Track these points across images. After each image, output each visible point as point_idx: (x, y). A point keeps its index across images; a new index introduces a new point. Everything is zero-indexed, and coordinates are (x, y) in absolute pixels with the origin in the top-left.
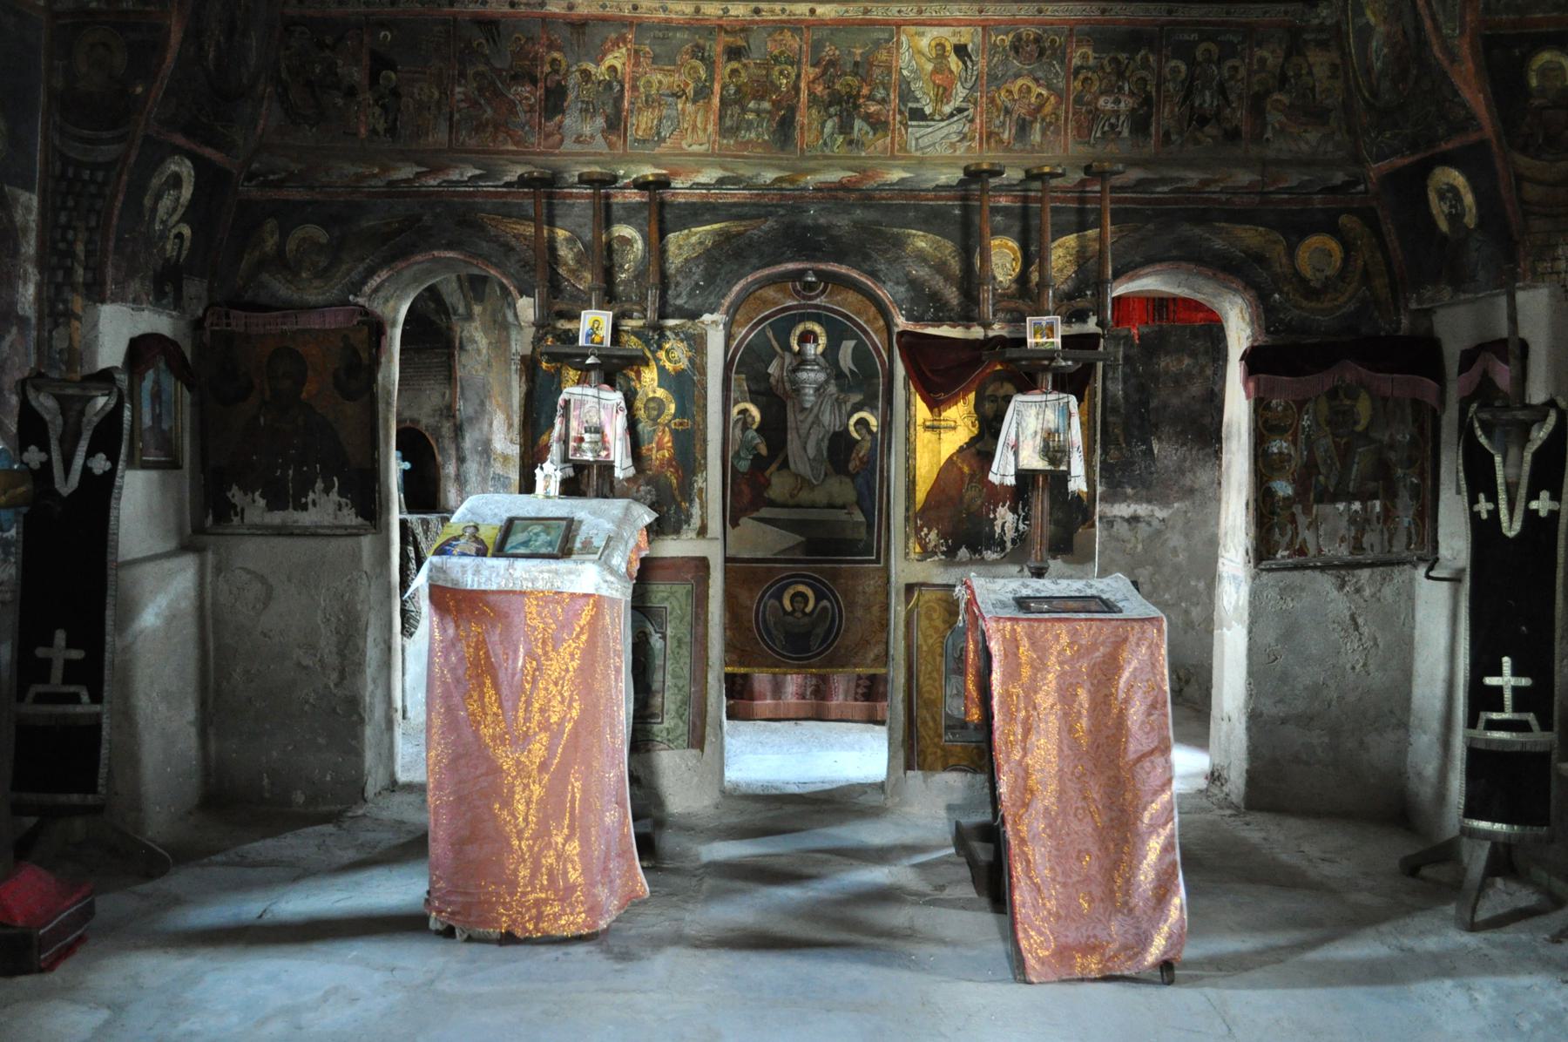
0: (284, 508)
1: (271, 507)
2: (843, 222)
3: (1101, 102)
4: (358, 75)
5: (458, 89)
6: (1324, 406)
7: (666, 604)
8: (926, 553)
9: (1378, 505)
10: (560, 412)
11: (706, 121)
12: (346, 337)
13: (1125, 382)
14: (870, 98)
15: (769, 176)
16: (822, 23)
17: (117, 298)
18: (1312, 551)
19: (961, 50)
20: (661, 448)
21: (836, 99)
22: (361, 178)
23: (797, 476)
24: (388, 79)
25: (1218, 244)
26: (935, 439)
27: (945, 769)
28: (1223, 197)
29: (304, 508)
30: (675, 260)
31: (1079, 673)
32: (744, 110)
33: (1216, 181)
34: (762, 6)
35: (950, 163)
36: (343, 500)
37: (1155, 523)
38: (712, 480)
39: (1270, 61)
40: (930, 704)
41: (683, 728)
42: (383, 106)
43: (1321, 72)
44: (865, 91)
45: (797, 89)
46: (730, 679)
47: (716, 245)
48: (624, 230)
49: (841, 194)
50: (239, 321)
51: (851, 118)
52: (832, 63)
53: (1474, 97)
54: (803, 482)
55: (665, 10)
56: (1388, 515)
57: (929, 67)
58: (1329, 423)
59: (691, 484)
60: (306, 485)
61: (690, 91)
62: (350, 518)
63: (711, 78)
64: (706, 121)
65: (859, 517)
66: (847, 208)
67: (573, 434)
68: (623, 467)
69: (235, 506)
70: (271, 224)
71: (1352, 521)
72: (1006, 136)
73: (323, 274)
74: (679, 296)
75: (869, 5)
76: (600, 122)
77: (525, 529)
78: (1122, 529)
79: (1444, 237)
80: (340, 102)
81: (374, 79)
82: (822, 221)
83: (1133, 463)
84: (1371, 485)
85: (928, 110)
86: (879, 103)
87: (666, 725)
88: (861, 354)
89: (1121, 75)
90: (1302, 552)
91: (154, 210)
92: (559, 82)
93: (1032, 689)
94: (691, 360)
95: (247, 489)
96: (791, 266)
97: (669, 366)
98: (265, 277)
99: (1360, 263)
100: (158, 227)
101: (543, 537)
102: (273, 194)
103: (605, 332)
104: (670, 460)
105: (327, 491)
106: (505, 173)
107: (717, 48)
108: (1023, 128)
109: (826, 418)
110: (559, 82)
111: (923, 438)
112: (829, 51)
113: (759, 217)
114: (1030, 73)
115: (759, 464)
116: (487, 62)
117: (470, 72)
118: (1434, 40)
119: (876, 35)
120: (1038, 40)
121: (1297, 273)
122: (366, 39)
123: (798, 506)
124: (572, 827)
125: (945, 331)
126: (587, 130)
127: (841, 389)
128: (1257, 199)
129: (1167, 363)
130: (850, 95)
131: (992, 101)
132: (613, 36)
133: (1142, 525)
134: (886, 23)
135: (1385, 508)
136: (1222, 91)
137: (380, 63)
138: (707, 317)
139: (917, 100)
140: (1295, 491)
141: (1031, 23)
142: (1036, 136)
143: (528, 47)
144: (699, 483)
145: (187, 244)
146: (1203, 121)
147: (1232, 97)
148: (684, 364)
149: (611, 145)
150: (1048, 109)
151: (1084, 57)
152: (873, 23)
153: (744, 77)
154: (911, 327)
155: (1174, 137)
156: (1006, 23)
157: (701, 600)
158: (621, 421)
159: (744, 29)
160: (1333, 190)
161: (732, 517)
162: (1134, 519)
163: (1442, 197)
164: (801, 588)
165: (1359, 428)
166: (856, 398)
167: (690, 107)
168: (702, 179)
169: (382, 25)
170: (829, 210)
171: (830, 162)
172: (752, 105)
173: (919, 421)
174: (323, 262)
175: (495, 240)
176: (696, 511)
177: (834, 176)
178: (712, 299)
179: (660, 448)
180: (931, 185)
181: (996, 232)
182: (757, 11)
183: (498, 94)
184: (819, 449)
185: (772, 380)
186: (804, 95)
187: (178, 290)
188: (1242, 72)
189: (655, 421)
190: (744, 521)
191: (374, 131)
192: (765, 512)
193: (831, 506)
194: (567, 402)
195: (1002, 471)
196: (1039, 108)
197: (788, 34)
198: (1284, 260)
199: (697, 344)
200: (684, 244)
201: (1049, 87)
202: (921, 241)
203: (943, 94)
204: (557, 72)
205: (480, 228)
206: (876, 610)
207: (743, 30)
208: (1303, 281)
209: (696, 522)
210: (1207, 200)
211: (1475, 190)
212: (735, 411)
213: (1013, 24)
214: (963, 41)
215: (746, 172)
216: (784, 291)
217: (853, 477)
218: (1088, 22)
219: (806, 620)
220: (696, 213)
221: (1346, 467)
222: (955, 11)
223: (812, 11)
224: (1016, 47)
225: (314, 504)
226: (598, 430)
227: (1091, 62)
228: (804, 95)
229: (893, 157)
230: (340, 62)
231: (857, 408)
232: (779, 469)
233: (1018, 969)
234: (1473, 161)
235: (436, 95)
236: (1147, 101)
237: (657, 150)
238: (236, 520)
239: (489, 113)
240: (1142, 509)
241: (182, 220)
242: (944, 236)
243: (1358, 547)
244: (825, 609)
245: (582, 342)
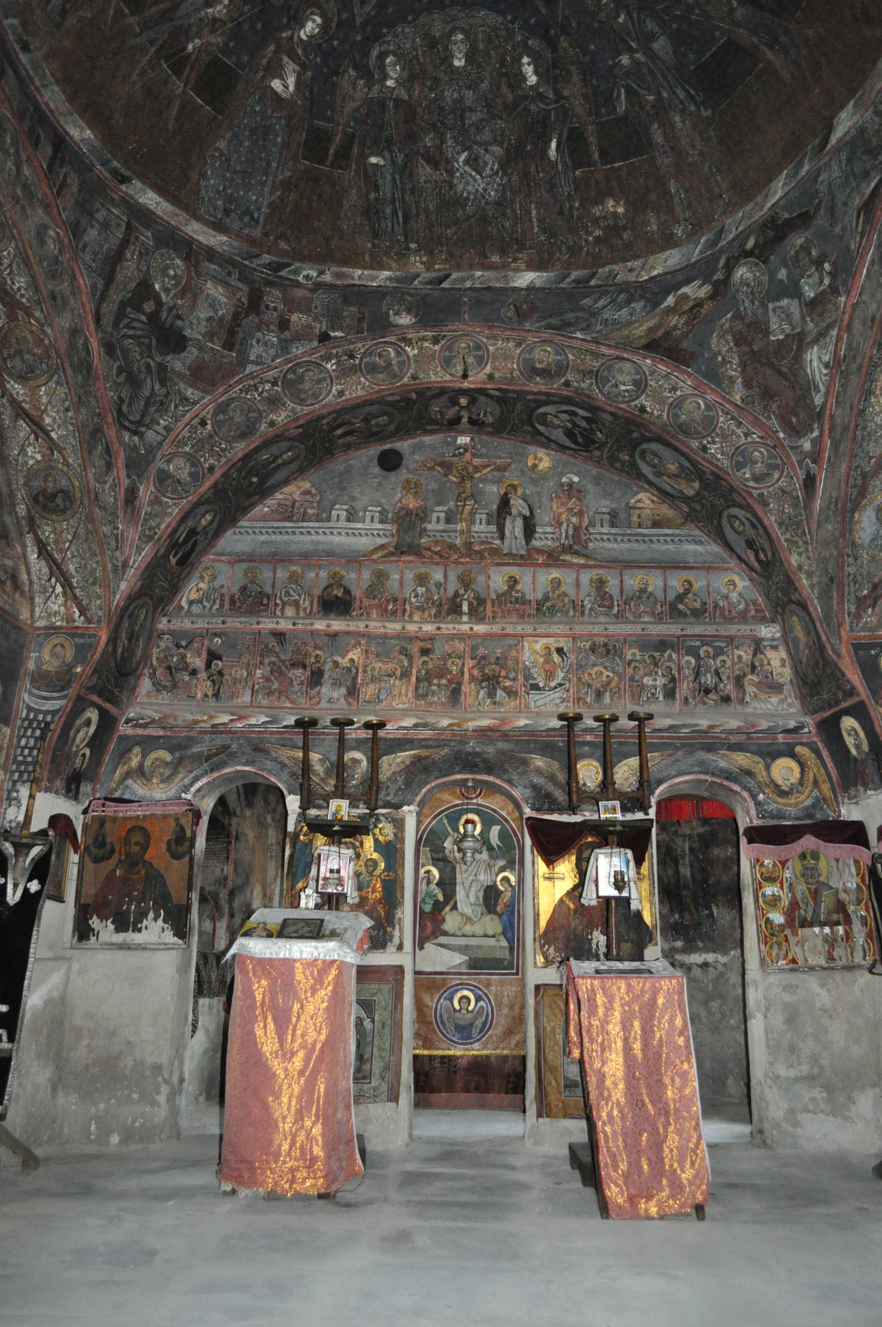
0: (126, 931)
1: (118, 930)
2: (490, 750)
3: (645, 680)
4: (198, 662)
5: (258, 671)
6: (799, 866)
7: (375, 998)
8: (548, 963)
9: (841, 930)
10: (315, 861)
11: (407, 692)
12: (177, 820)
13: (691, 867)
14: (506, 677)
15: (445, 722)
16: (477, 636)
17: (47, 790)
18: (801, 961)
19: (560, 651)
21: (486, 678)
22: (197, 722)
23: (462, 915)
24: (217, 665)
25: (722, 764)
26: (550, 887)
27: (565, 1117)
28: (723, 736)
29: (140, 930)
31: (631, 1011)
32: (430, 684)
33: (718, 726)
34: (443, 626)
36: (166, 926)
37: (720, 967)
38: (406, 913)
39: (745, 657)
40: (553, 1069)
41: (384, 1088)
42: (213, 681)
43: (776, 663)
44: (503, 673)
45: (462, 672)
46: (416, 1057)
47: (413, 763)
49: (489, 733)
50: (111, 809)
51: (495, 689)
52: (483, 658)
53: (854, 677)
54: (468, 919)
55: (384, 627)
56: (848, 936)
57: (541, 660)
58: (803, 876)
59: (394, 915)
60: (143, 915)
61: (398, 673)
62: (169, 937)
63: (411, 665)
64: (407, 692)
65: (504, 943)
66: (492, 742)
67: (322, 875)
68: (353, 897)
69: (93, 930)
70: (137, 750)
71: (825, 939)
72: (589, 700)
73: (166, 780)
74: (388, 794)
75: (505, 626)
76: (343, 691)
77: (295, 924)
78: (697, 972)
79: (855, 758)
80: (187, 678)
81: (208, 665)
82: (478, 749)
83: (700, 924)
84: (835, 917)
85: (541, 685)
86: (511, 680)
87: (373, 1084)
88: (503, 835)
89: (656, 665)
90: (794, 961)
91: (74, 739)
92: (319, 668)
93: (605, 1022)
94: (395, 834)
95: (103, 918)
96: (459, 777)
97: (381, 838)
98: (129, 782)
99: (811, 775)
100: (74, 749)
101: (306, 929)
102: (140, 731)
104: (380, 899)
105: (155, 919)
106: (283, 720)
107: (415, 649)
108: (599, 695)
110: (319, 668)
111: (543, 886)
112: (481, 651)
113: (439, 747)
114: (602, 664)
115: (438, 907)
116: (277, 656)
117: (267, 661)
118: (828, 647)
119: (508, 642)
120: (605, 645)
121: (772, 781)
122: (206, 643)
123: (464, 936)
124: (317, 1115)
125: (555, 817)
126: (335, 695)
127: (492, 857)
128: (744, 736)
129: (716, 852)
130: (494, 676)
131: (580, 679)
132: (353, 642)
133: (711, 969)
134: (515, 636)
135: (847, 933)
136: (717, 674)
137: (213, 656)
138: (406, 808)
139: (534, 679)
140: (786, 920)
141: (602, 636)
142: (607, 699)
143: (302, 648)
144: (399, 915)
145: (87, 760)
146: (707, 691)
147: (724, 678)
148: (391, 837)
149: (349, 704)
150: (614, 684)
151: (634, 654)
152: (508, 635)
153: (430, 666)
154: (534, 814)
155: (690, 700)
156: (587, 635)
157: (398, 996)
159: (431, 638)
160: (789, 731)
161: (420, 943)
162: (705, 965)
163: (849, 734)
164: (466, 993)
165: (822, 879)
166: (501, 863)
167: (398, 682)
168: (404, 724)
169: (216, 635)
170: (482, 743)
171: (483, 714)
172: (435, 681)
173: (541, 874)
174: (167, 774)
175: (275, 760)
176: (397, 933)
177: (485, 723)
178: (409, 797)
180: (544, 728)
181: (584, 756)
182: (439, 629)
183: (281, 673)
184: (477, 897)
185: (447, 851)
186: (466, 676)
187: (78, 788)
188: (729, 663)
189: (371, 874)
190: (427, 945)
191: (206, 695)
192: (442, 940)
193: (486, 936)
194: (319, 855)
195: (589, 898)
196: (608, 684)
197: (457, 641)
198: (764, 773)
199: (399, 824)
200: (392, 764)
201: (613, 672)
202: (539, 762)
203: (550, 675)
204: (318, 662)
205: (266, 752)
206: (517, 1007)
207: (430, 639)
208: (777, 786)
209: (396, 941)
210: (713, 737)
211: (864, 729)
212: (422, 871)
213: (591, 636)
214: (561, 645)
215: (431, 720)
216: (453, 794)
217: (500, 916)
218: (635, 635)
219: (470, 1015)
220: (398, 745)
221: (817, 903)
222: (555, 629)
223: (471, 629)
224: (593, 649)
225: (146, 928)
227: (638, 658)
228: (466, 676)
229: (521, 712)
230: (189, 655)
231: (502, 869)
232: (451, 910)
233: (604, 1209)
234: (860, 712)
235: (245, 674)
236: (673, 680)
237: (378, 707)
238: (93, 939)
239: (276, 685)
240: (710, 957)
241: (87, 746)
242: (553, 758)
243: (831, 958)
244: (482, 1007)
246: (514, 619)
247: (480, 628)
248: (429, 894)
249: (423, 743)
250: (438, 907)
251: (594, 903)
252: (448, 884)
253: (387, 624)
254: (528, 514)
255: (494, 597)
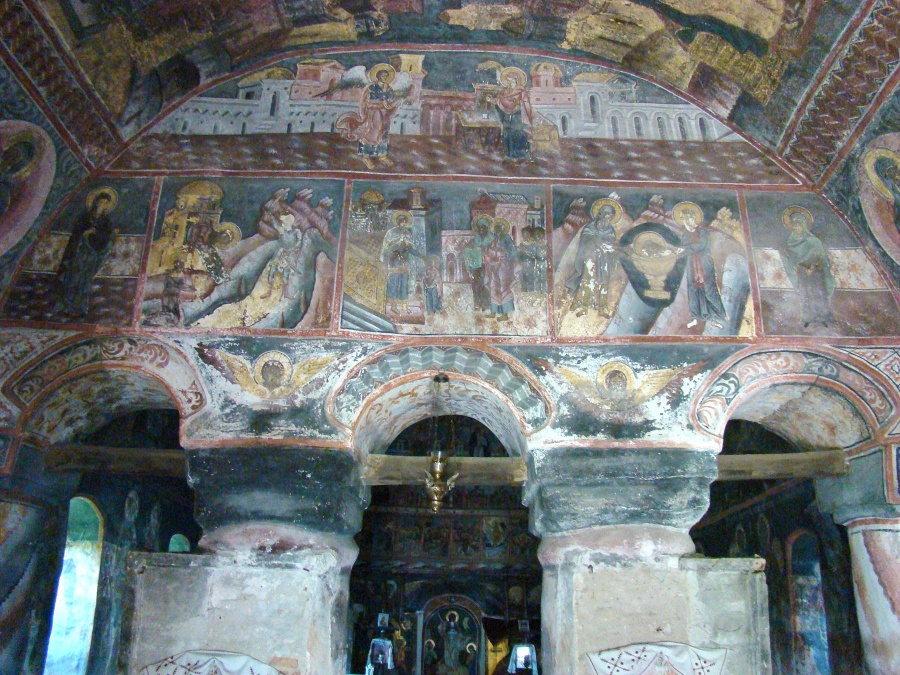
2: (464, 580)
15: (439, 565)
16: (457, 515)
20: (402, 656)
30: (407, 593)
35: (498, 562)
48: (392, 582)
54: (451, 669)
61: (414, 536)
88: (471, 623)
94: (412, 627)
103: (386, 621)
109: (459, 646)
148: (409, 628)
158: (390, 651)
179: (401, 656)
186: (451, 538)
189: (399, 648)
199: (414, 621)
200: (412, 586)
202: (490, 587)
212: (426, 642)
215: (433, 564)
217: (468, 667)
226: (383, 653)
231: (470, 641)
245: (379, 624)
246: (477, 506)
247: (459, 512)
248: (429, 655)
249: (428, 577)
250: (435, 662)
251: (514, 672)
252: (440, 650)
253: (409, 509)
254: (486, 444)
255: (467, 493)
